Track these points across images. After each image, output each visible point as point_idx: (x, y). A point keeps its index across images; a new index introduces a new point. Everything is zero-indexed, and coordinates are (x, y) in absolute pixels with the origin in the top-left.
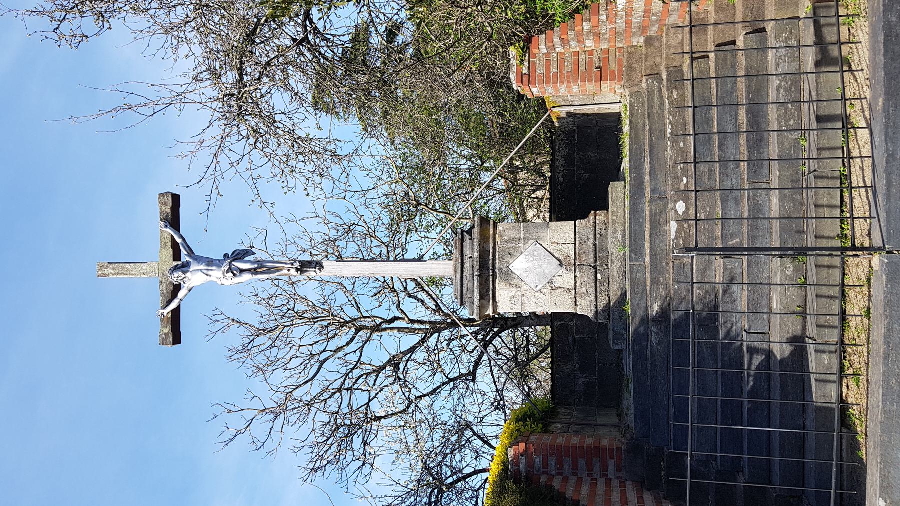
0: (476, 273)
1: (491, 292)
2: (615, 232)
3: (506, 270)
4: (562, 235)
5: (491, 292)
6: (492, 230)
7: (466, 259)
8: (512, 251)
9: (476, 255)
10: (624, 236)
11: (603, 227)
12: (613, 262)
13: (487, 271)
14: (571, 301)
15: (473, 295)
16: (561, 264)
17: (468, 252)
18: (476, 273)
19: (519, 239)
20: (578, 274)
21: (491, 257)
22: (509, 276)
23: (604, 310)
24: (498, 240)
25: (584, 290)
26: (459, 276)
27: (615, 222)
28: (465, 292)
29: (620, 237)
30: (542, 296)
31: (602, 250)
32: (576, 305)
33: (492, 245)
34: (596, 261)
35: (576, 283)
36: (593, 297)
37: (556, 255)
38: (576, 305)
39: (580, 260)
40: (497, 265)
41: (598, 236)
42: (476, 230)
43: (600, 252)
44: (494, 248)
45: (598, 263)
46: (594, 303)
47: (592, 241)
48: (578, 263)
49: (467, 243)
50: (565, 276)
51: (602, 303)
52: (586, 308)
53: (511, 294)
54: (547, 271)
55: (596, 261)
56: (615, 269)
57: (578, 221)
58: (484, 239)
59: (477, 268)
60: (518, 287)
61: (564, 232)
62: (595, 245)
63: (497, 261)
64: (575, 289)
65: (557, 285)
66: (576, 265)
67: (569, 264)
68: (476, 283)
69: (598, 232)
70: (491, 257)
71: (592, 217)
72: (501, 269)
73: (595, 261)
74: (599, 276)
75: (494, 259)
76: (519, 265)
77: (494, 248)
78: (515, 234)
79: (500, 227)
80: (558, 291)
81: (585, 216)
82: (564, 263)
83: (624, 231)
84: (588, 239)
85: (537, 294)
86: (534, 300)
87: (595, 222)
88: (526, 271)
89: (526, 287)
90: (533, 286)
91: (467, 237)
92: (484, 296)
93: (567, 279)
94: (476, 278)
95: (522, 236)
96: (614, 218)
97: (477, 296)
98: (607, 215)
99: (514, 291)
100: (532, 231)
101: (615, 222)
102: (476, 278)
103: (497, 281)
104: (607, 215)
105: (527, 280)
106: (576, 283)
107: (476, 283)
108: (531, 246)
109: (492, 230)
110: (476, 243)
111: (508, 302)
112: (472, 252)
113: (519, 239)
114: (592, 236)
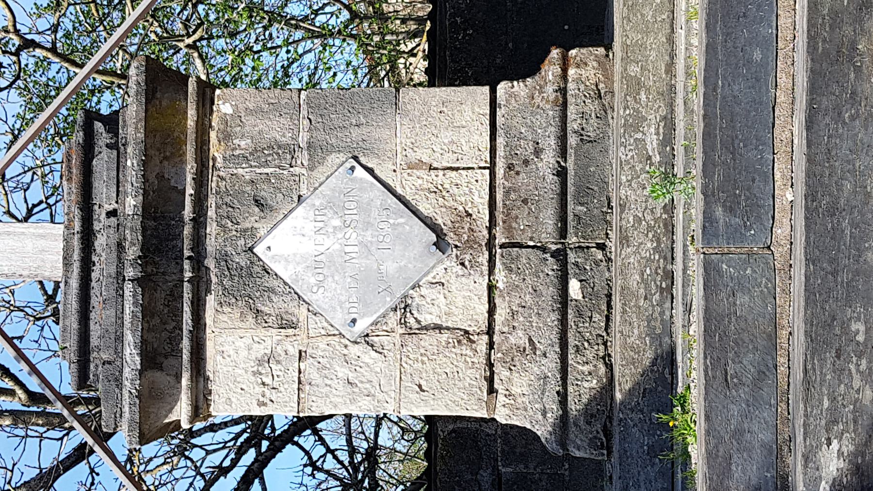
0: (130, 272)
1: (186, 344)
2: (635, 124)
3: (242, 260)
4: (446, 136)
5: (186, 344)
6: (192, 113)
7: (100, 222)
8: (265, 192)
9: (131, 203)
10: (667, 140)
11: (592, 107)
12: (624, 240)
13: (167, 265)
14: (475, 376)
15: (119, 353)
16: (441, 244)
17: (104, 197)
18: (130, 272)
19: (292, 150)
20: (501, 277)
21: (188, 212)
22: (252, 282)
23: (589, 414)
24: (216, 150)
25: (519, 338)
26: (74, 283)
27: (635, 86)
28: (94, 341)
29: (652, 142)
30: (369, 356)
31: (584, 193)
32: (492, 390)
33: (190, 168)
34: (563, 233)
35: (491, 311)
36: (551, 364)
37: (425, 209)
38: (492, 390)
39: (509, 229)
40: (212, 244)
41: (572, 140)
42: (133, 112)
43: (579, 198)
44: (201, 181)
45: (572, 240)
46: (554, 386)
47: (549, 158)
48: (500, 239)
49: (103, 162)
50: (454, 284)
51: (584, 387)
52: (524, 403)
53: (260, 350)
54: (390, 267)
55: (563, 233)
56: (631, 263)
57: (502, 88)
58: (162, 145)
59: (132, 252)
60: (287, 324)
61: (449, 130)
62: (562, 173)
63: (212, 228)
64: (490, 332)
65: (427, 319)
66: (496, 246)
67: (471, 244)
68: (128, 308)
69: (573, 125)
70: (188, 212)
71: (550, 70)
72: (224, 258)
73: (556, 233)
74: (574, 288)
75: (200, 221)
76: (288, 244)
77: (201, 181)
78: (276, 129)
79: (223, 107)
80: (429, 340)
81: (526, 67)
82: (451, 238)
83: (669, 123)
84: (538, 152)
85: (355, 350)
86: (343, 372)
87: (563, 91)
88: (317, 265)
89: (316, 325)
90: (339, 319)
91: (103, 137)
92: (156, 356)
93: (459, 295)
94: (128, 287)
95: (303, 138)
96: (634, 70)
97: (132, 356)
98: (605, 65)
99: (271, 338)
100: (336, 120)
101: (635, 86)
102: (128, 287)
103: (211, 301)
104: (605, 65)
105: (317, 299)
106: (491, 311)
107: (128, 308)
108: (337, 178)
109: (192, 113)
110: (131, 163)
111: (247, 380)
112: (122, 197)
113: (292, 150)
114: (550, 144)
